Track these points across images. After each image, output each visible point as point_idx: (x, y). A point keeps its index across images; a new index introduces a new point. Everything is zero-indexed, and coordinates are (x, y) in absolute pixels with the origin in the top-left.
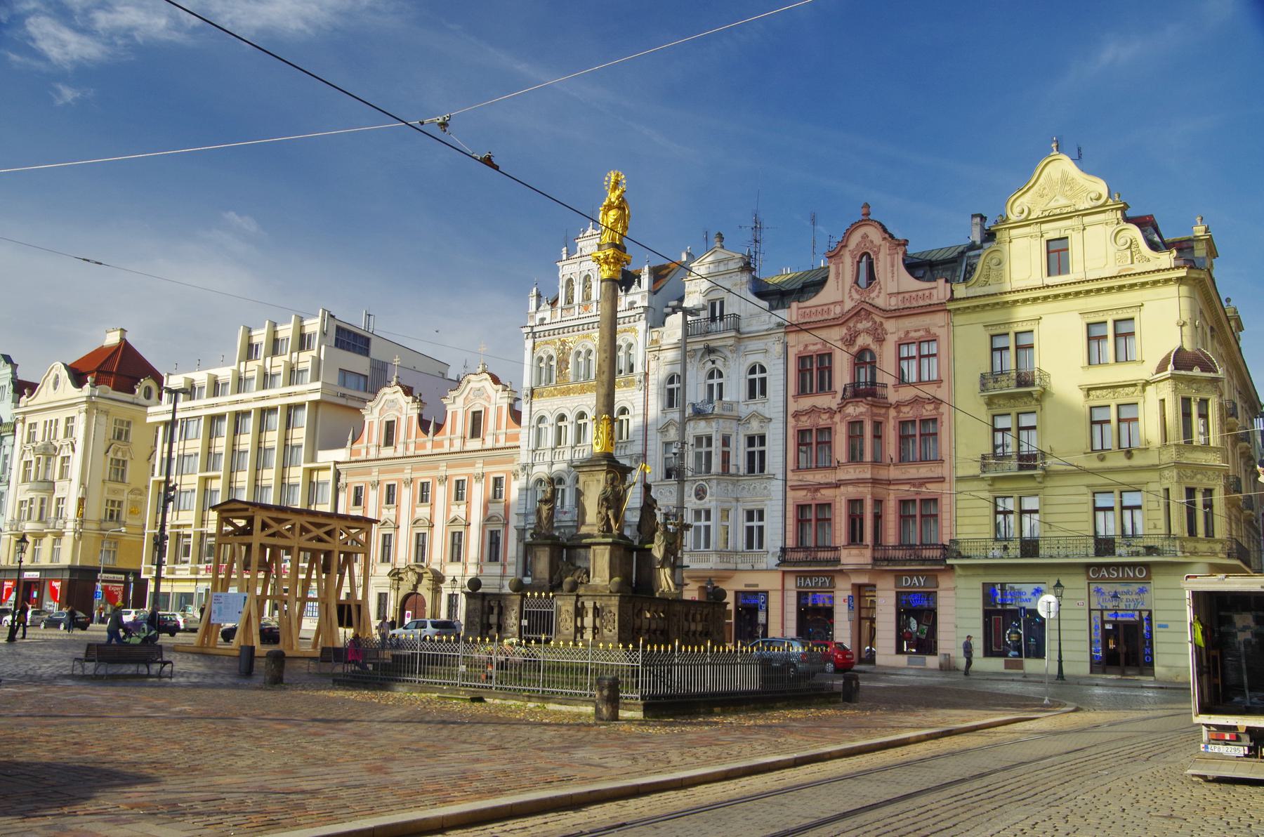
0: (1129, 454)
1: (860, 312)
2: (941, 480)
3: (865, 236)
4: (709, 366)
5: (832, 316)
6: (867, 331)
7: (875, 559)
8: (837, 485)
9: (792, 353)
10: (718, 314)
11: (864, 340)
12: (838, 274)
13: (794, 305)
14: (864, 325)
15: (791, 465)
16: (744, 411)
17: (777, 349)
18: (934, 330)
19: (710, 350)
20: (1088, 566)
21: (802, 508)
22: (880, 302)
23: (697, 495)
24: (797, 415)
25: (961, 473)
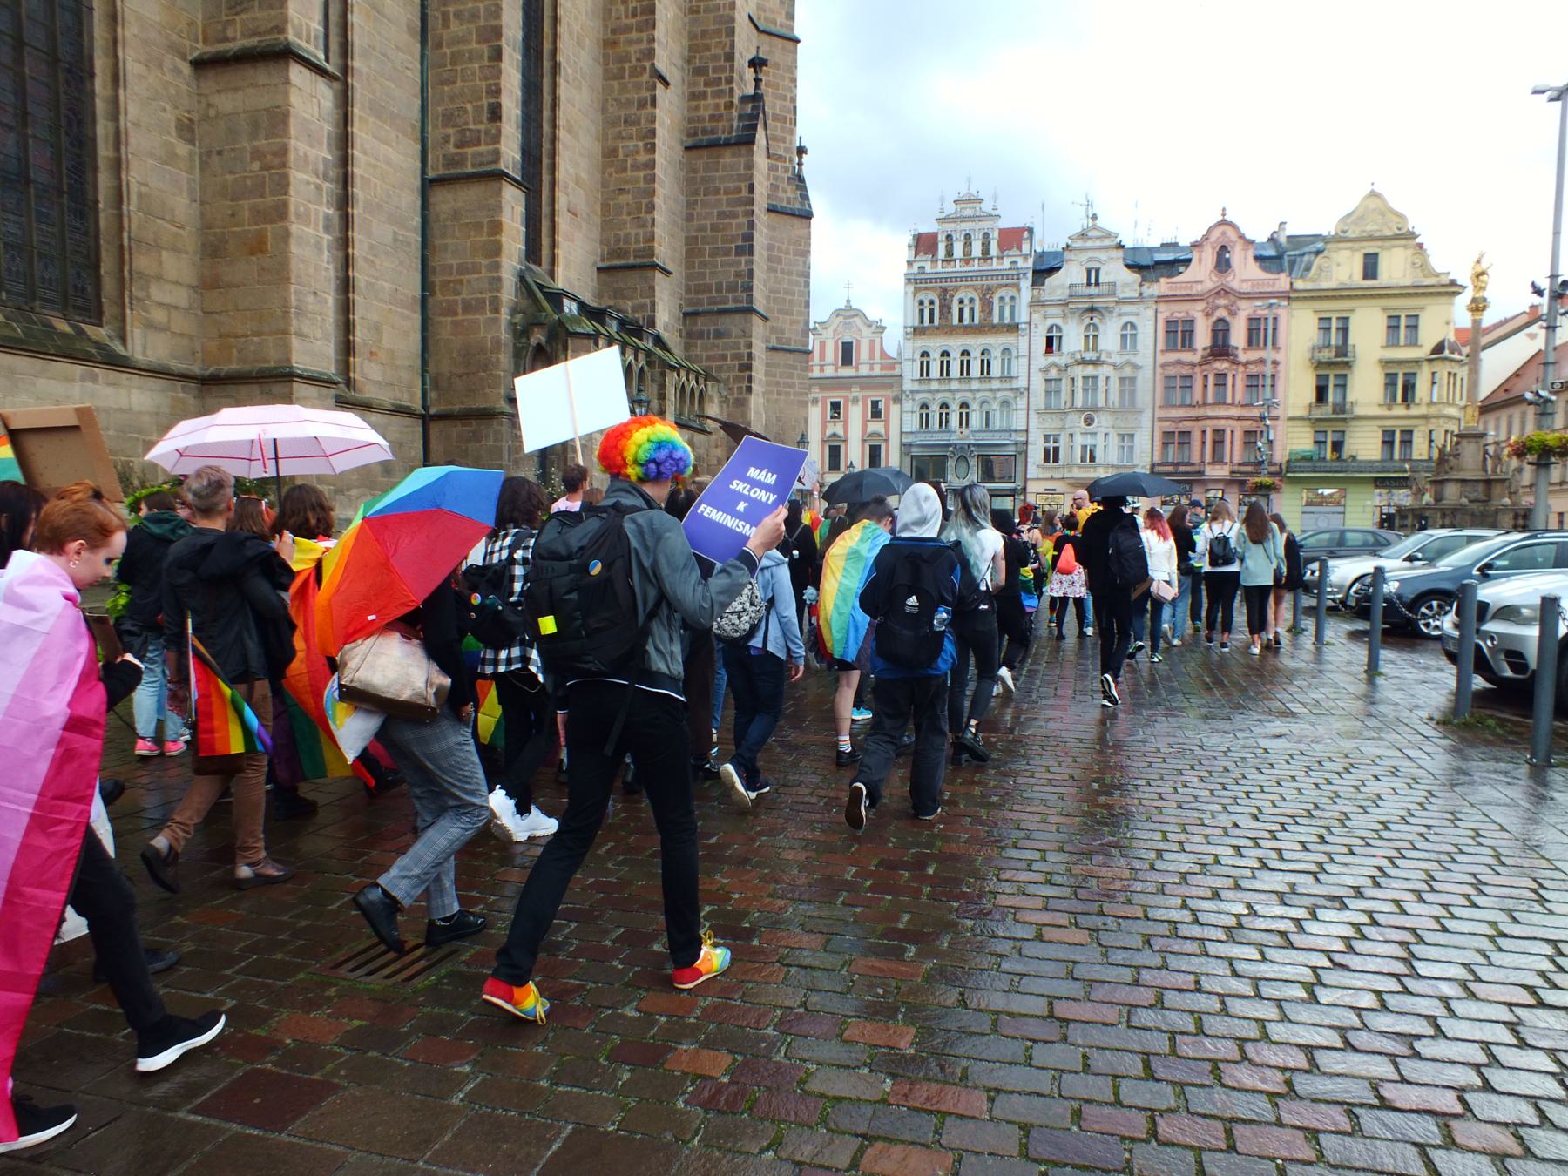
0: (1408, 407)
1: (1223, 292)
3: (1224, 233)
4: (1087, 321)
6: (1226, 307)
9: (1161, 318)
13: (1163, 280)
14: (1222, 301)
15: (1158, 403)
16: (1116, 359)
17: (1150, 313)
19: (1092, 309)
21: (1167, 434)
22: (1235, 285)
24: (1164, 366)
25: (1291, 414)
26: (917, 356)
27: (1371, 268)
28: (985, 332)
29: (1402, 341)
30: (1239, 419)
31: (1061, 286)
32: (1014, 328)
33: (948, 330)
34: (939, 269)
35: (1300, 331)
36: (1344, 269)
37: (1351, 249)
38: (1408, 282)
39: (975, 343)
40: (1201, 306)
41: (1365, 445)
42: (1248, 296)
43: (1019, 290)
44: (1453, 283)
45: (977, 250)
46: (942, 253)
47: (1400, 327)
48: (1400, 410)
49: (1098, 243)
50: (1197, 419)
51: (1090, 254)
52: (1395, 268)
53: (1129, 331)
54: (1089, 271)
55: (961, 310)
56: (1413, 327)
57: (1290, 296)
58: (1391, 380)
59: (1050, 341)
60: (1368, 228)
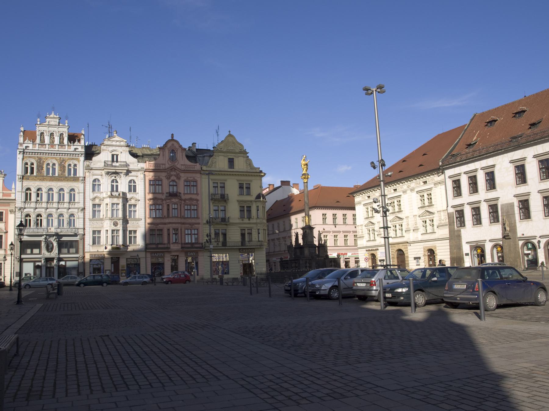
1: (173, 169)
2: (199, 224)
3: (173, 145)
5: (161, 168)
7: (182, 248)
8: (165, 224)
10: (115, 160)
11: (173, 178)
12: (163, 155)
18: (196, 178)
20: (240, 249)
22: (178, 166)
23: (114, 224)
26: (24, 190)
27: (231, 162)
28: (61, 180)
29: (245, 194)
30: (183, 224)
31: (100, 162)
32: (76, 179)
33: (42, 178)
34: (37, 148)
35: (205, 186)
36: (221, 163)
37: (224, 156)
38: (245, 170)
39: (56, 185)
40: (164, 174)
41: (234, 236)
42: (184, 171)
43: (79, 161)
44: (261, 172)
45: (57, 140)
46: (38, 141)
47: (245, 188)
48: (246, 221)
49: (118, 143)
50: (165, 224)
51: (114, 148)
52: (240, 164)
53: (132, 184)
54: (113, 156)
55: (48, 170)
56: (248, 188)
57: (201, 172)
58: (242, 211)
59: (94, 186)
60: (229, 148)
